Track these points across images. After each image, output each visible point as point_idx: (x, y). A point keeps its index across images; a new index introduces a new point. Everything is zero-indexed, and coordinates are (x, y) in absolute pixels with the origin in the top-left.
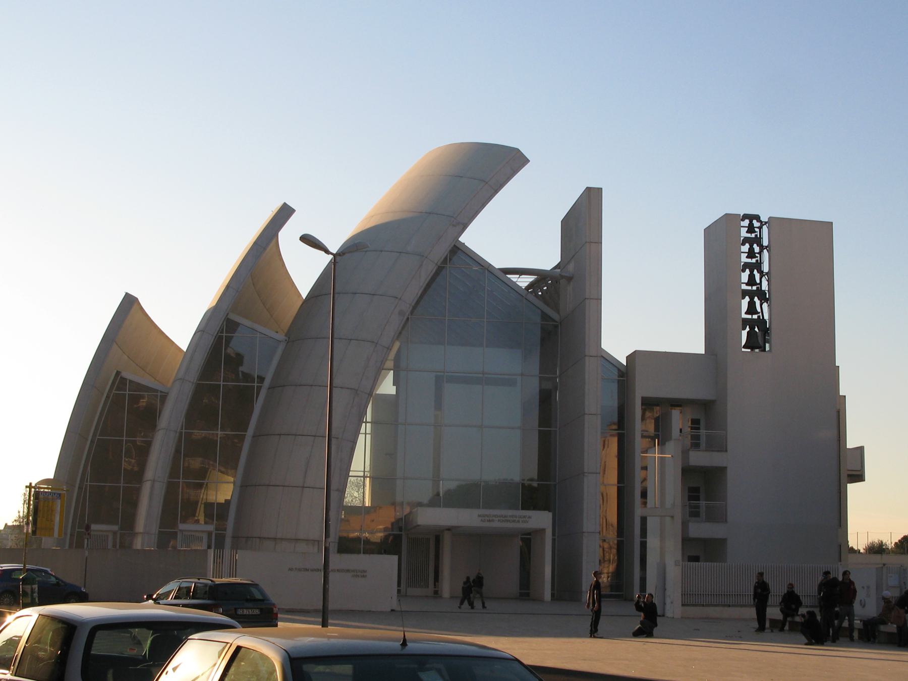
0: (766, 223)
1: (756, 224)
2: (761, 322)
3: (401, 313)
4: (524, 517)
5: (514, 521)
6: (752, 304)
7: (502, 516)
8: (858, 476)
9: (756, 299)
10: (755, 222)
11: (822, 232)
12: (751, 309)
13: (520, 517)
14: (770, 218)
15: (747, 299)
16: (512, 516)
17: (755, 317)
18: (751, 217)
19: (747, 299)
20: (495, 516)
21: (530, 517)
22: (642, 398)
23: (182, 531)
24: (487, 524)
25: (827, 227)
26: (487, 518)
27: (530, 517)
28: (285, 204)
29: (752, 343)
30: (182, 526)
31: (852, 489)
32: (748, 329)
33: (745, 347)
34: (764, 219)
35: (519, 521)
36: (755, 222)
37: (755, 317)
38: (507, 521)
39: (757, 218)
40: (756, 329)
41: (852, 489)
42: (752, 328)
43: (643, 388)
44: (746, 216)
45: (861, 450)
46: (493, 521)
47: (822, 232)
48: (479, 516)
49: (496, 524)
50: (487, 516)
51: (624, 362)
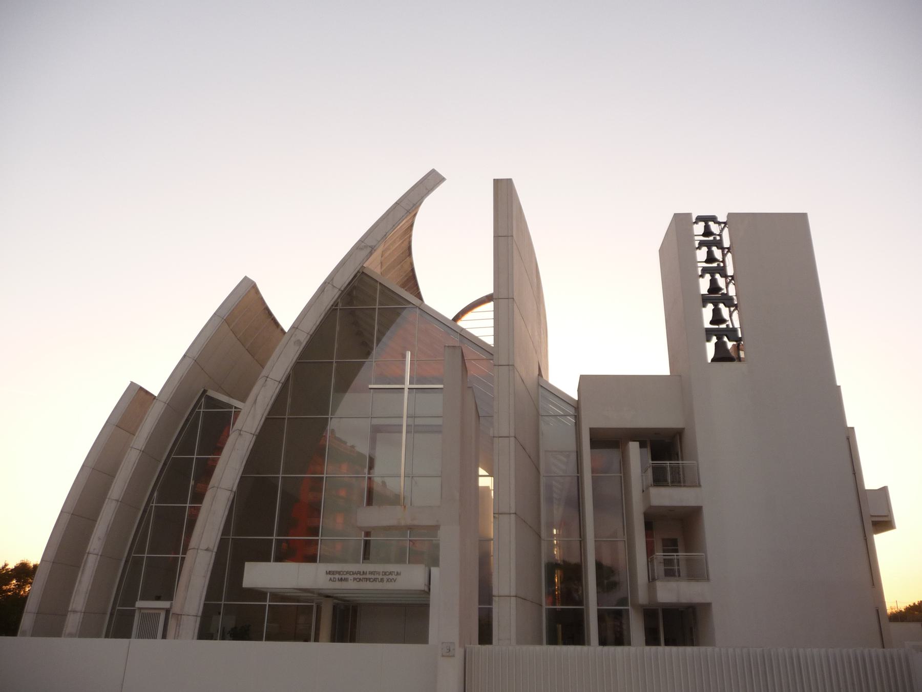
0: (725, 223)
1: (715, 228)
2: (731, 333)
3: (298, 342)
4: (391, 573)
5: (375, 580)
6: (716, 312)
7: (359, 573)
8: (885, 523)
9: (721, 306)
10: (711, 224)
11: (794, 228)
12: (717, 318)
13: (385, 573)
14: (730, 215)
15: (710, 307)
16: (371, 573)
17: (723, 326)
18: (706, 219)
19: (710, 307)
20: (348, 573)
21: (398, 574)
22: (593, 431)
23: (140, 609)
24: (338, 585)
25: (800, 221)
26: (337, 576)
27: (398, 574)
28: (246, 277)
29: (722, 355)
30: (140, 604)
31: (881, 540)
32: (714, 339)
33: (713, 360)
34: (722, 218)
35: (382, 580)
36: (711, 224)
37: (723, 326)
38: (367, 579)
39: (713, 219)
40: (725, 339)
41: (881, 540)
42: (719, 338)
43: (592, 420)
44: (700, 219)
45: (883, 492)
46: (346, 580)
47: (794, 228)
48: (329, 573)
49: (351, 585)
50: (339, 573)
51: (576, 397)
